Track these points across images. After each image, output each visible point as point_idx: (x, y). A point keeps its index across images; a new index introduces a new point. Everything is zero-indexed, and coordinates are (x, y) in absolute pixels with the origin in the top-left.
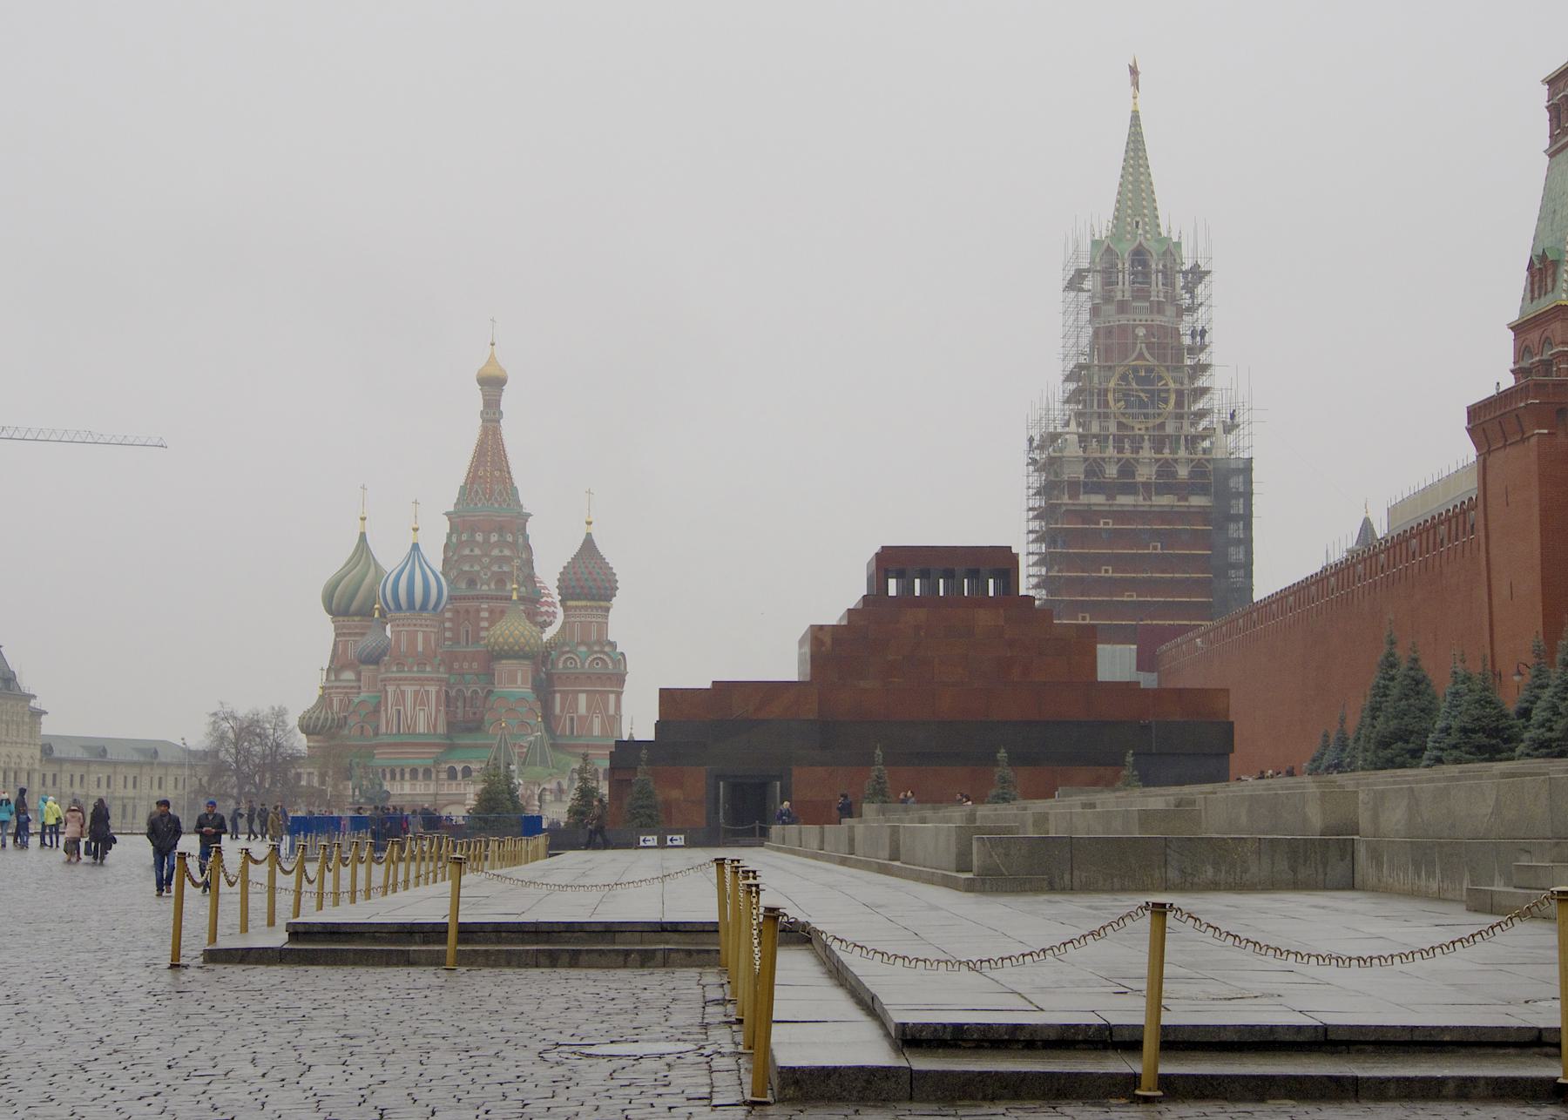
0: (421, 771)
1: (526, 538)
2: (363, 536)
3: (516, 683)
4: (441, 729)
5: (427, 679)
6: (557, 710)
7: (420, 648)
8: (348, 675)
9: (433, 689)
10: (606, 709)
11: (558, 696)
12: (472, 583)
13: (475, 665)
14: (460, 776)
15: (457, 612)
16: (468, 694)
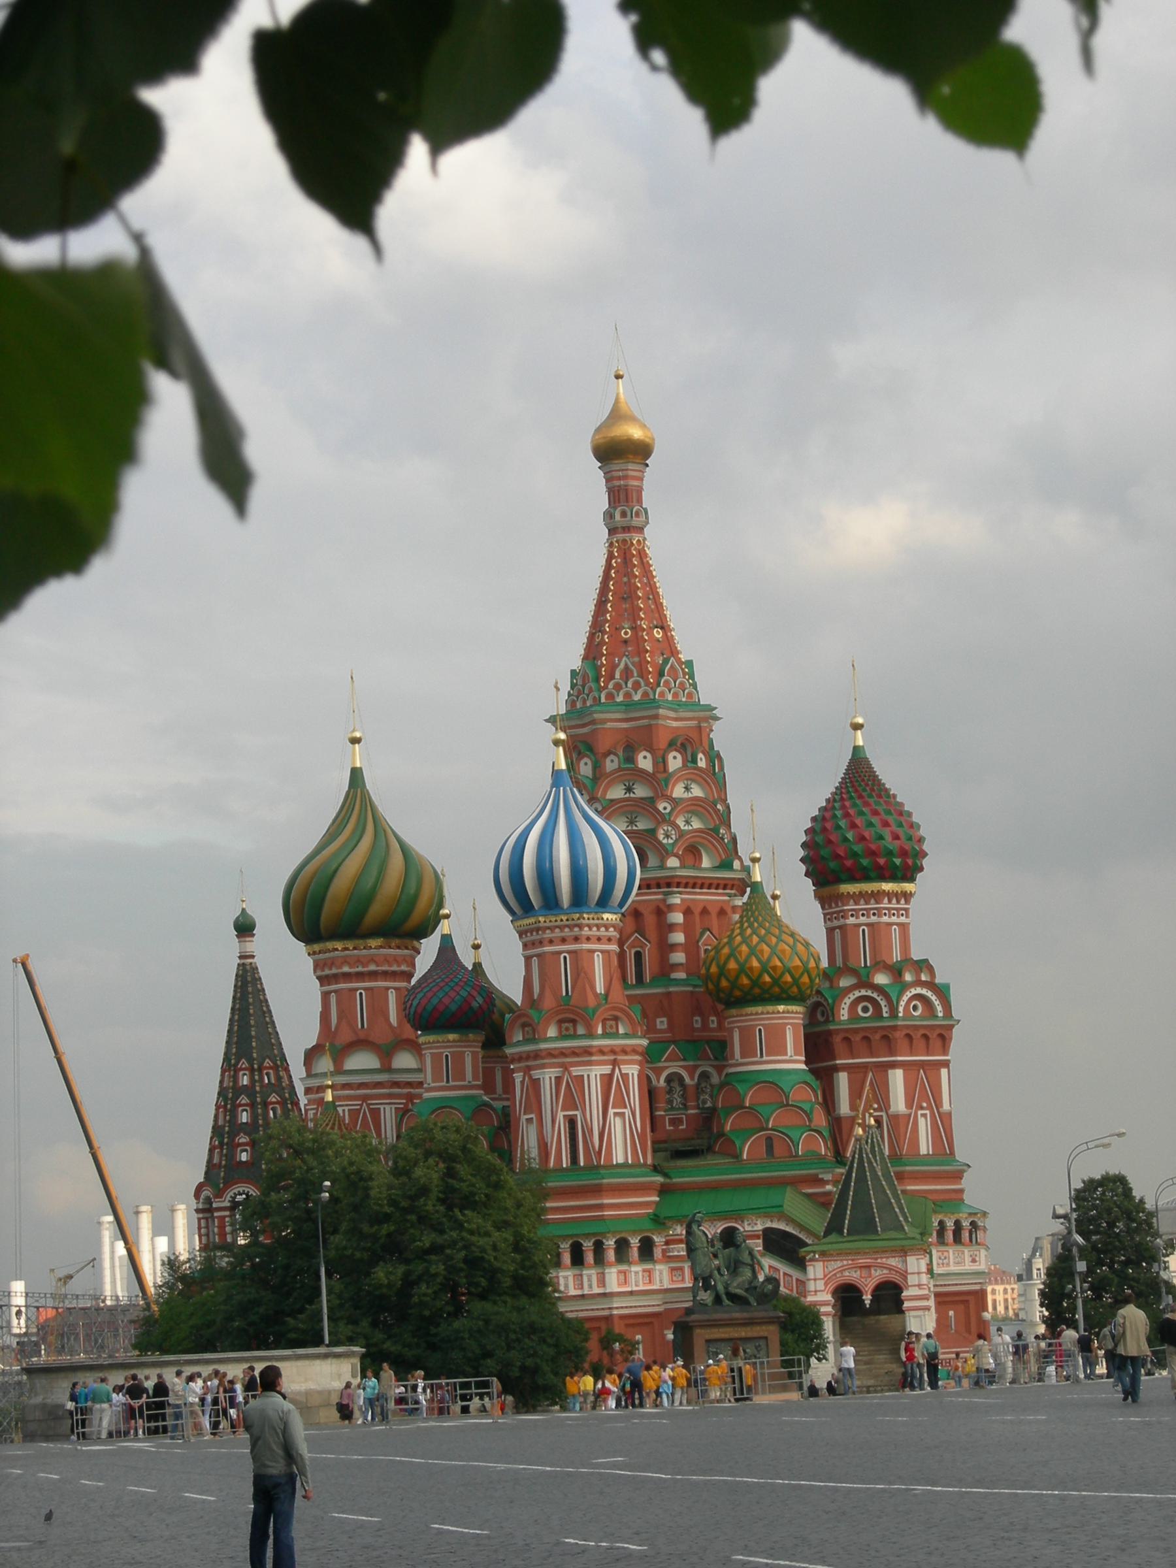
0: (635, 1242)
2: (356, 775)
6: (844, 1108)
7: (600, 988)
8: (363, 1061)
9: (632, 1070)
10: (939, 1104)
11: (843, 1079)
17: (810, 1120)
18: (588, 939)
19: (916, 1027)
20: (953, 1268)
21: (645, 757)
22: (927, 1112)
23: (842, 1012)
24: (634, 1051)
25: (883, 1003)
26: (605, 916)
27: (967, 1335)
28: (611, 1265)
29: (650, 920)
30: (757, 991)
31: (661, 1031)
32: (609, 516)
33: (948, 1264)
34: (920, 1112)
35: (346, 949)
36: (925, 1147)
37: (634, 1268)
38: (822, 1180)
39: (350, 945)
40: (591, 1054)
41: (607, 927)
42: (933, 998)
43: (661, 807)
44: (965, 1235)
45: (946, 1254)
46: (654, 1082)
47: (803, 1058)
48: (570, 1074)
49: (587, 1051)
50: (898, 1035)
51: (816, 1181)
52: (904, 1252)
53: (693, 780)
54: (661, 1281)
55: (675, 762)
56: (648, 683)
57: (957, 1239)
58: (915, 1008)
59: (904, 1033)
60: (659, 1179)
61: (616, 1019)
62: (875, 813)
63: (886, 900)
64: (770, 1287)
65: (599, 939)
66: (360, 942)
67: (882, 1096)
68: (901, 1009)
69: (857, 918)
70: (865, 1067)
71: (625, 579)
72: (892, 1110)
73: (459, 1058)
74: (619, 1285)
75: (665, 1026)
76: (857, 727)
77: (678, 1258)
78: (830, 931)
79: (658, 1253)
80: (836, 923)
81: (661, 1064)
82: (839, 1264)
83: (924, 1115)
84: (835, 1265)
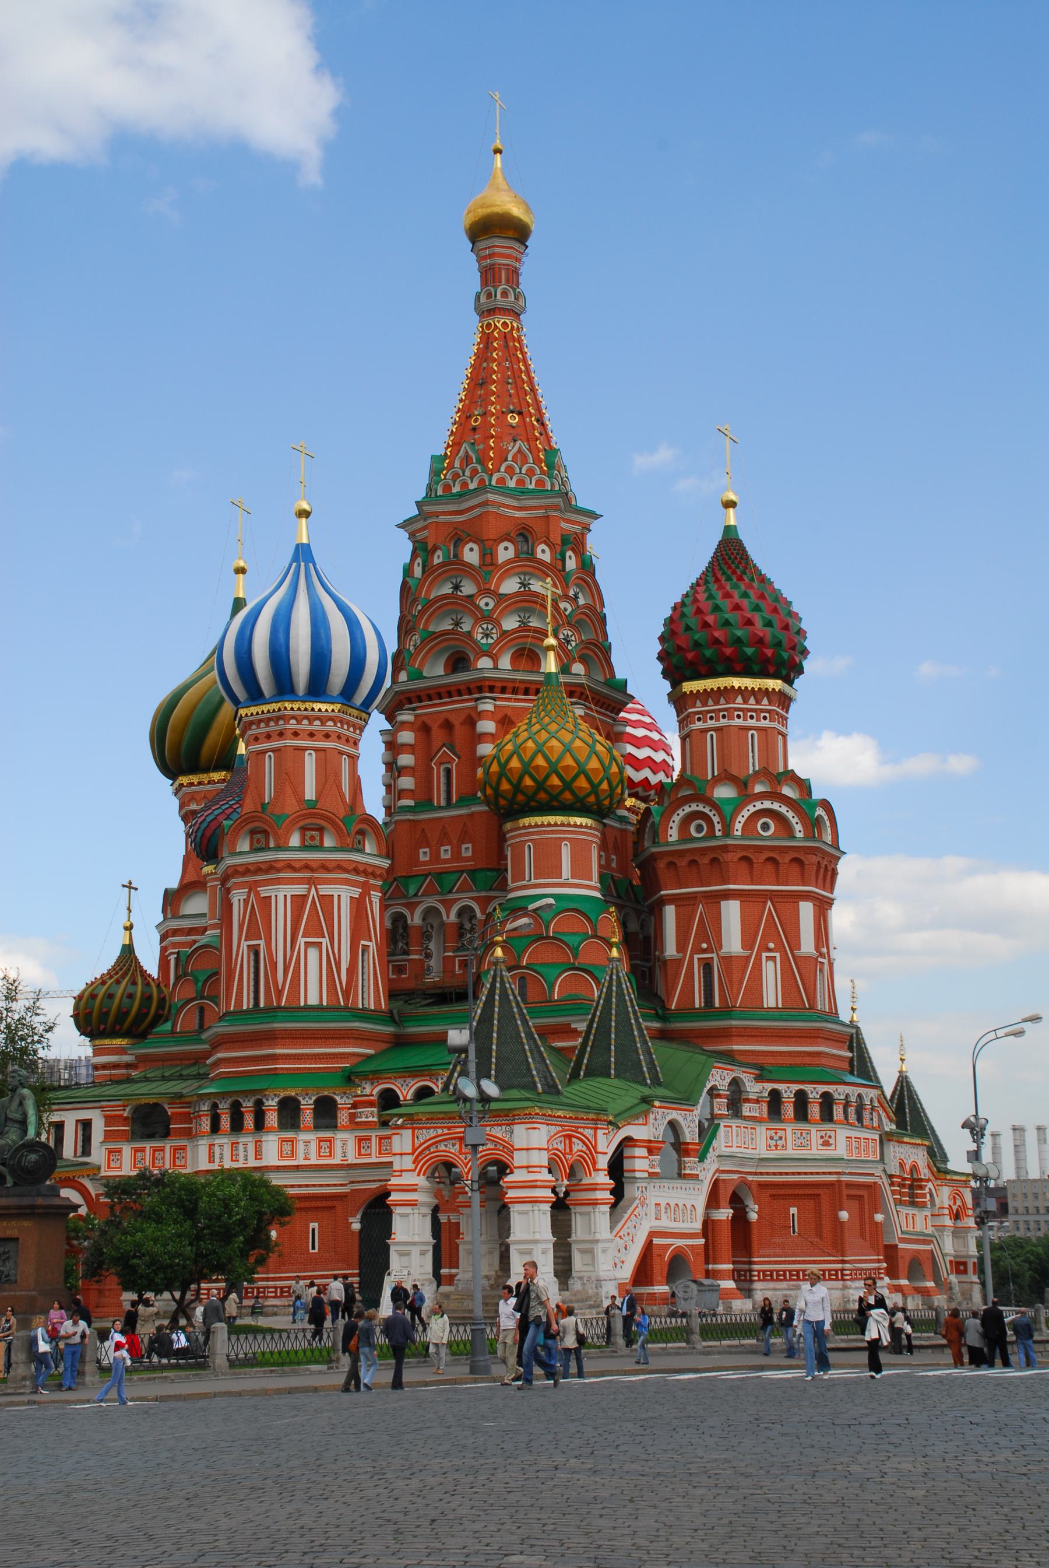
0: (307, 1103)
3: (563, 869)
5: (324, 867)
6: (671, 949)
7: (310, 793)
9: (344, 894)
10: (795, 942)
11: (670, 912)
13: (467, 850)
15: (423, 729)
17: (575, 958)
18: (296, 734)
19: (759, 849)
20: (790, 1152)
21: (471, 550)
22: (777, 955)
23: (670, 832)
24: (340, 867)
25: (716, 819)
26: (317, 706)
27: (816, 1240)
28: (271, 1130)
29: (459, 730)
30: (520, 798)
31: (467, 859)
33: (784, 1147)
34: (764, 955)
35: (191, 784)
36: (771, 996)
37: (303, 1136)
38: (575, 1031)
39: (195, 778)
40: (279, 871)
41: (323, 720)
42: (790, 815)
43: (482, 604)
44: (814, 1111)
45: (781, 1133)
46: (445, 918)
47: (595, 882)
48: (257, 894)
49: (271, 867)
50: (732, 857)
51: (567, 1031)
53: (532, 575)
54: (344, 1154)
55: (505, 553)
56: (486, 470)
59: (740, 854)
60: (391, 1029)
61: (321, 830)
62: (727, 595)
63: (739, 699)
64: (33, 1157)
65: (312, 735)
66: (205, 777)
68: (738, 827)
69: (705, 722)
70: (693, 898)
71: (485, 365)
72: (724, 950)
74: (281, 1156)
75: (469, 854)
76: (730, 504)
77: (367, 1125)
78: (683, 739)
79: (343, 1118)
80: (686, 730)
81: (451, 896)
82: (432, 1133)
83: (774, 959)
84: (425, 1135)
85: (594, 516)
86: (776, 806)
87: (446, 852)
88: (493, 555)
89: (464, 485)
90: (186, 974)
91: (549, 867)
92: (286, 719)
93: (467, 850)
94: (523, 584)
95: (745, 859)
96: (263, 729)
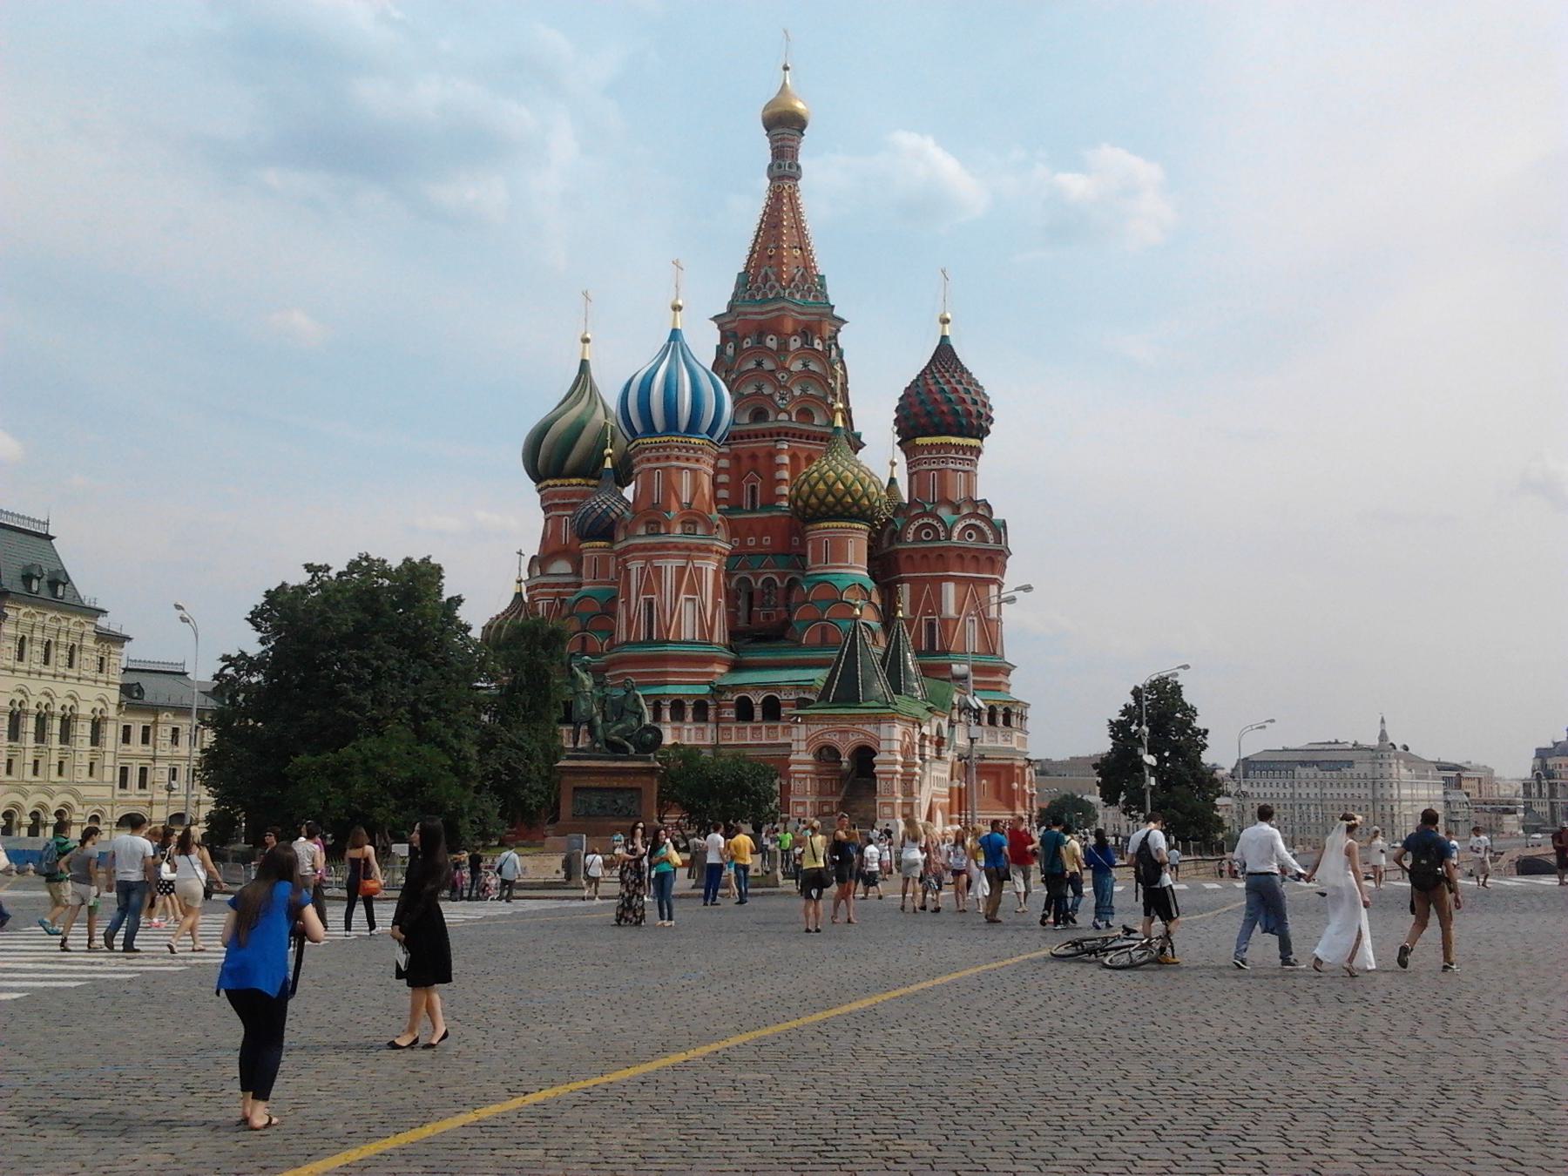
1: (840, 353)
2: (584, 365)
4: (720, 635)
5: (698, 548)
7: (685, 498)
8: (562, 567)
9: (710, 567)
11: (905, 591)
12: (759, 415)
13: (767, 540)
14: (758, 713)
15: (736, 458)
16: (758, 585)
18: (678, 458)
30: (823, 509)
32: (770, 167)
39: (558, 482)
42: (986, 529)
49: (664, 546)
52: (878, 720)
55: (795, 344)
57: (992, 722)
58: (970, 536)
61: (695, 523)
65: (688, 459)
66: (566, 482)
67: (936, 601)
73: (605, 560)
77: (728, 720)
78: (910, 476)
84: (816, 728)
85: (844, 322)
86: (978, 523)
87: (751, 541)
88: (786, 344)
89: (765, 294)
90: (571, 614)
91: (839, 553)
92: (672, 448)
93: (767, 540)
94: (805, 365)
95: (960, 556)
96: (654, 453)
